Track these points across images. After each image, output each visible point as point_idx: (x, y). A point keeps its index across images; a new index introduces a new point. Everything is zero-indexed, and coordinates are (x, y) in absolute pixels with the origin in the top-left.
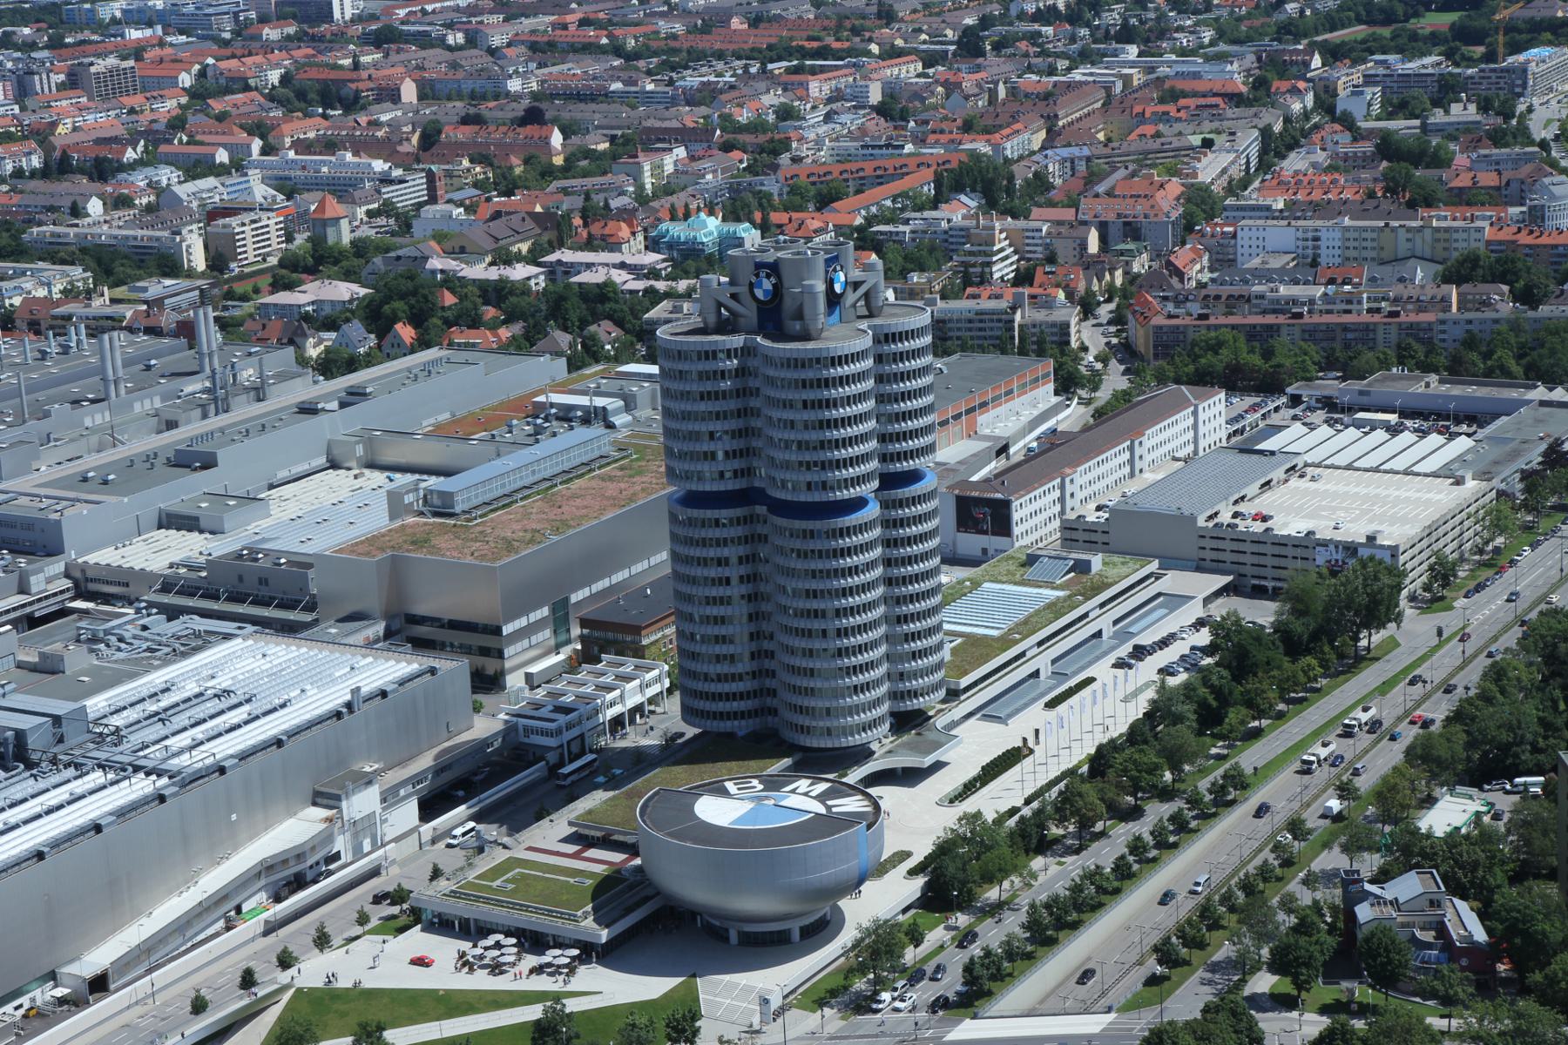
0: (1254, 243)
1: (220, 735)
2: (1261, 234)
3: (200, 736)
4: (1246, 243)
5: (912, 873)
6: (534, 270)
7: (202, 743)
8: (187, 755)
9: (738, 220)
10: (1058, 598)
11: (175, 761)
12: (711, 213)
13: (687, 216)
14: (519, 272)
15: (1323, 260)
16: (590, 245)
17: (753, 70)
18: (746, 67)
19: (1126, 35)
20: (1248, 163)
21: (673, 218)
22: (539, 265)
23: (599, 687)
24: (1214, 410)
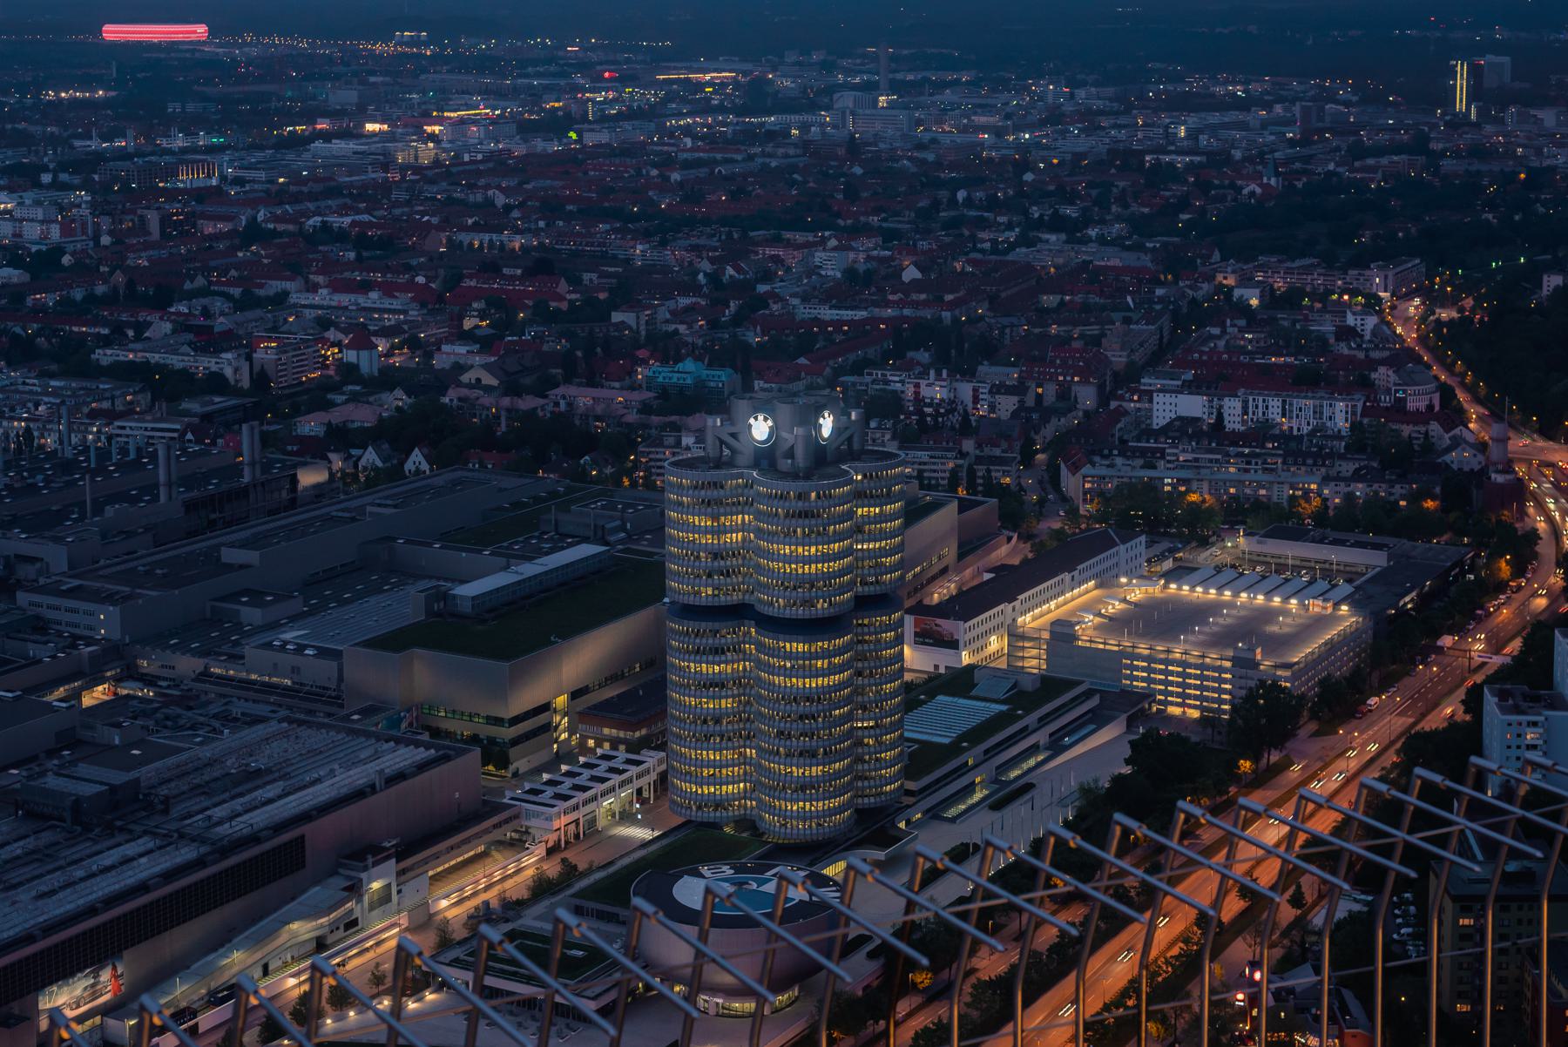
0: (1168, 407)
1: (256, 808)
2: (1173, 400)
3: (239, 808)
4: (1161, 407)
5: (872, 955)
6: (542, 401)
7: (239, 815)
8: (227, 825)
9: (722, 366)
10: (1002, 712)
11: (218, 829)
12: (698, 359)
13: (679, 359)
14: (527, 403)
15: (1229, 427)
16: (592, 383)
17: (736, 236)
18: (729, 234)
19: (1057, 224)
20: (1162, 337)
21: (664, 361)
22: (546, 397)
23: (594, 779)
24: (1136, 551)
